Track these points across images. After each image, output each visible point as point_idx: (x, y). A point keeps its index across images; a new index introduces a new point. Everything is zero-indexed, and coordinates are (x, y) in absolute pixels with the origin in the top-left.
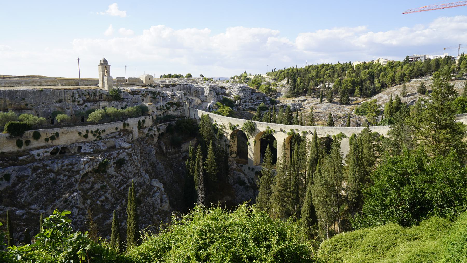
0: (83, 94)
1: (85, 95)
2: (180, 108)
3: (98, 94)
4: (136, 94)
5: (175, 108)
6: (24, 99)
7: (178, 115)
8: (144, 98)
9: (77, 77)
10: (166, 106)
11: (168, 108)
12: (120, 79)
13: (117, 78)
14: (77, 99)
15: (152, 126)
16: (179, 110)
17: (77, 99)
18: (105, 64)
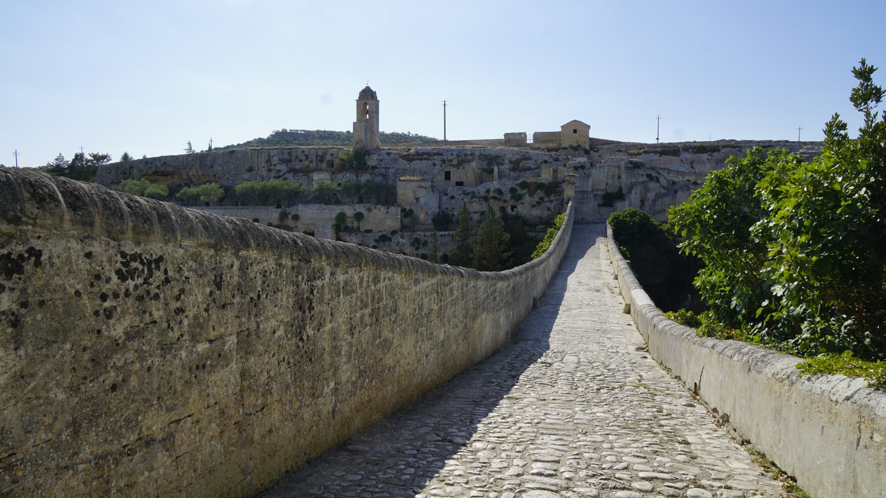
0: (297, 157)
1: (301, 161)
2: (552, 197)
3: (328, 157)
4: (426, 159)
5: (536, 198)
6: (212, 166)
7: (541, 218)
8: (452, 170)
9: (440, 138)
10: (513, 190)
11: (517, 198)
12: (511, 137)
13: (506, 135)
14: (275, 165)
15: (394, 232)
16: (547, 204)
17: (275, 165)
18: (368, 100)
